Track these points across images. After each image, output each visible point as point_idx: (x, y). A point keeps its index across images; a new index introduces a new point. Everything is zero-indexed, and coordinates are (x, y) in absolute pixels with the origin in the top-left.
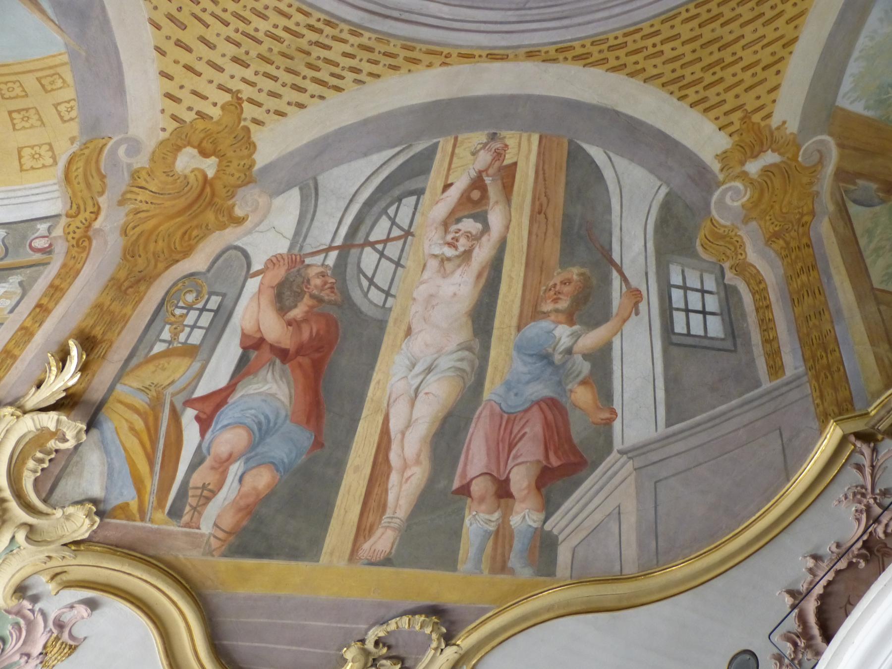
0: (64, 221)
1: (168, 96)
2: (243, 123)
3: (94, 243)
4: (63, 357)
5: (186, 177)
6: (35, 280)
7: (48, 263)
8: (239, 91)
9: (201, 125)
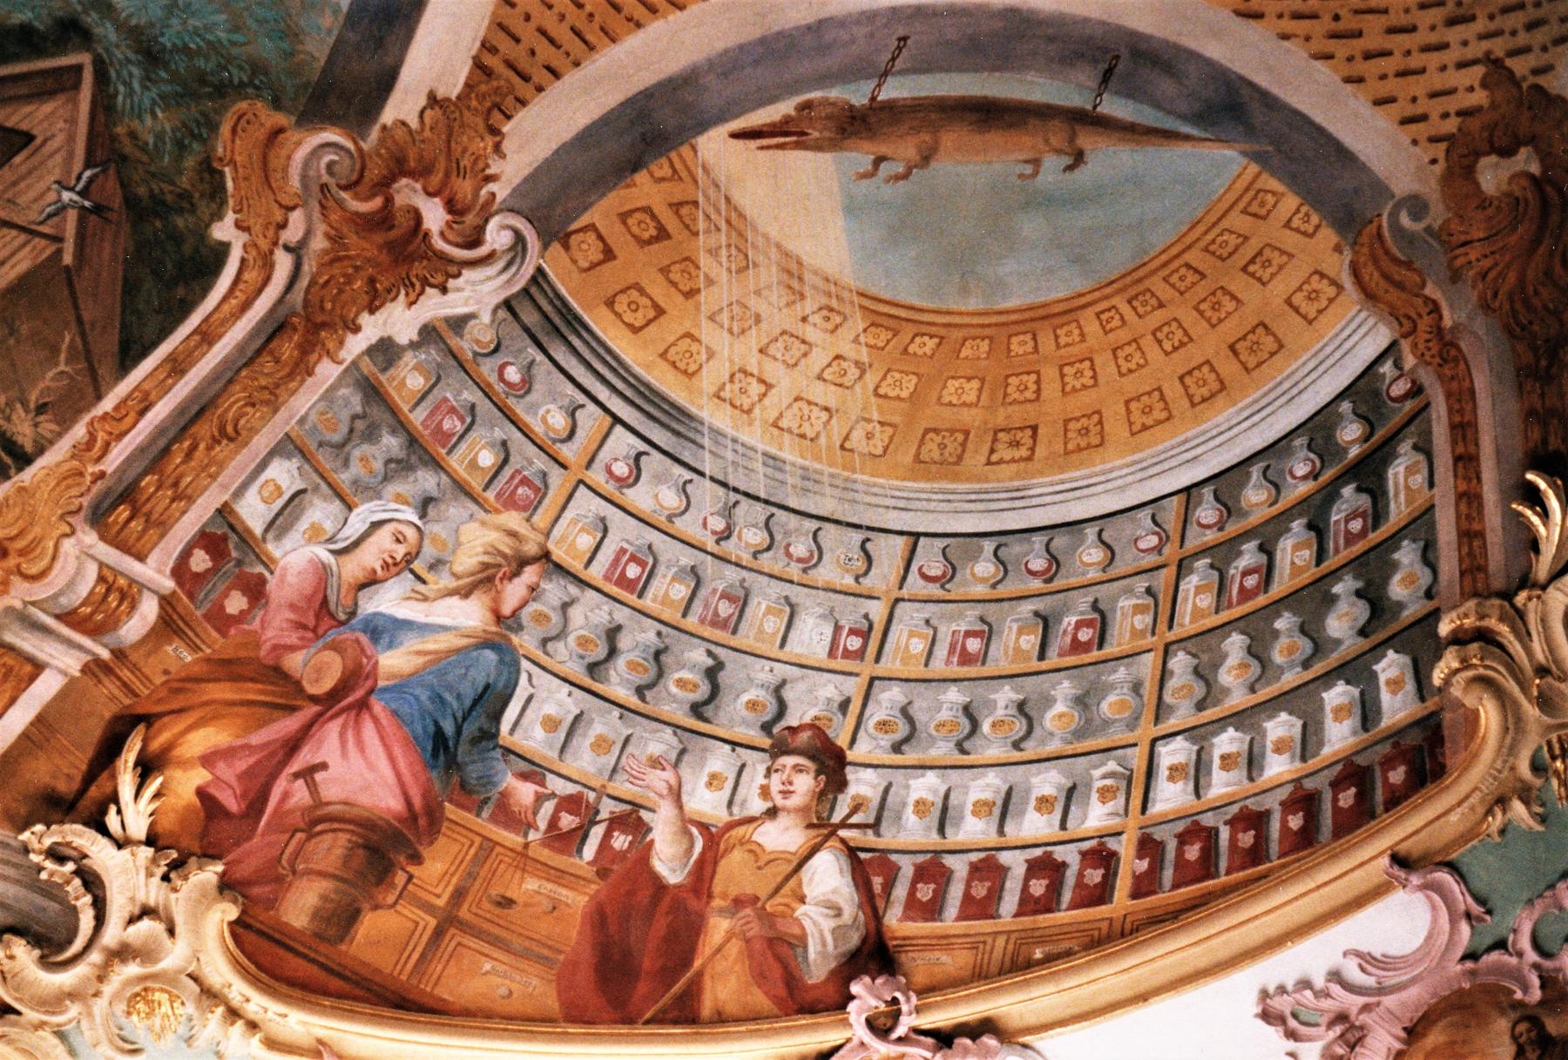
0: (1405, 346)
1: (1406, 121)
2: (1525, 86)
3: (1463, 345)
4: (1533, 498)
5: (1508, 195)
6: (1429, 433)
7: (1428, 405)
8: (1488, 53)
9: (1474, 124)
